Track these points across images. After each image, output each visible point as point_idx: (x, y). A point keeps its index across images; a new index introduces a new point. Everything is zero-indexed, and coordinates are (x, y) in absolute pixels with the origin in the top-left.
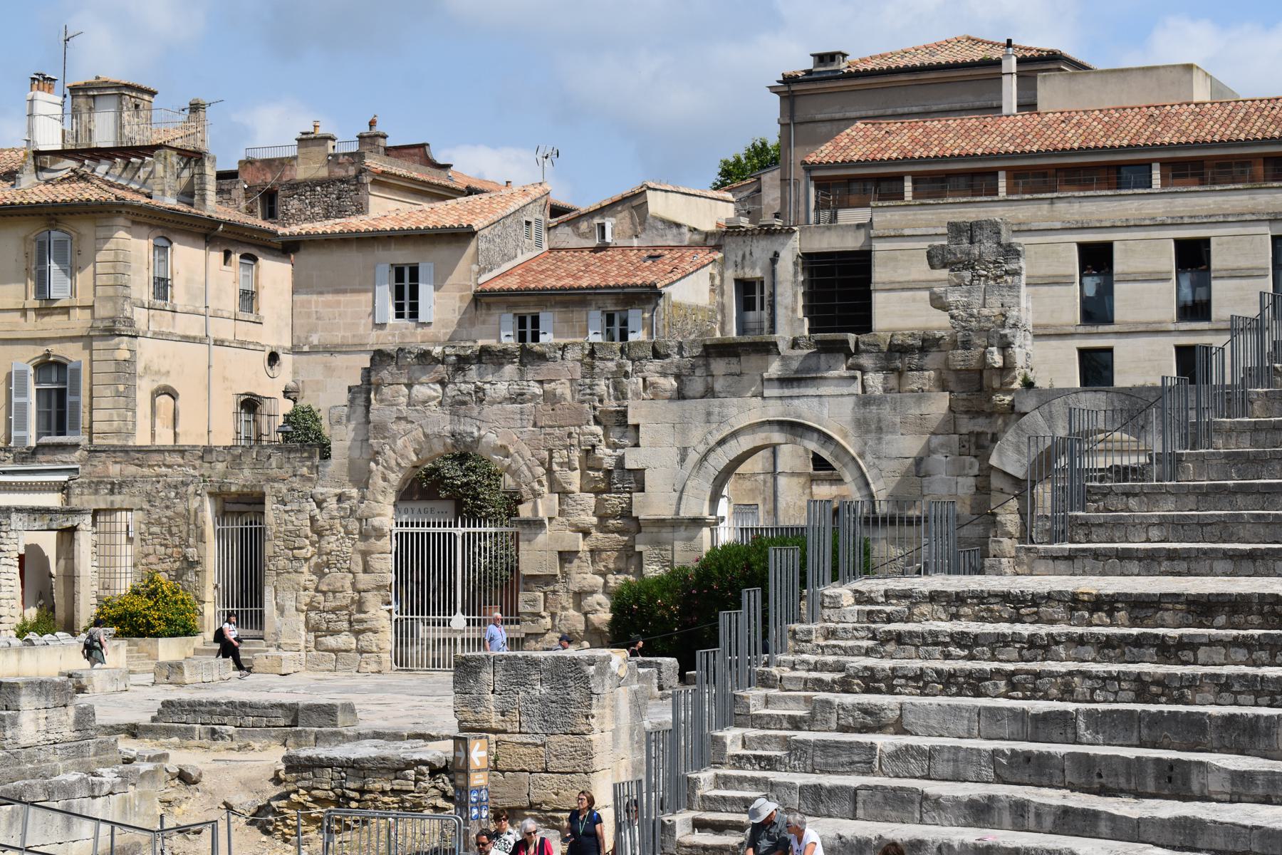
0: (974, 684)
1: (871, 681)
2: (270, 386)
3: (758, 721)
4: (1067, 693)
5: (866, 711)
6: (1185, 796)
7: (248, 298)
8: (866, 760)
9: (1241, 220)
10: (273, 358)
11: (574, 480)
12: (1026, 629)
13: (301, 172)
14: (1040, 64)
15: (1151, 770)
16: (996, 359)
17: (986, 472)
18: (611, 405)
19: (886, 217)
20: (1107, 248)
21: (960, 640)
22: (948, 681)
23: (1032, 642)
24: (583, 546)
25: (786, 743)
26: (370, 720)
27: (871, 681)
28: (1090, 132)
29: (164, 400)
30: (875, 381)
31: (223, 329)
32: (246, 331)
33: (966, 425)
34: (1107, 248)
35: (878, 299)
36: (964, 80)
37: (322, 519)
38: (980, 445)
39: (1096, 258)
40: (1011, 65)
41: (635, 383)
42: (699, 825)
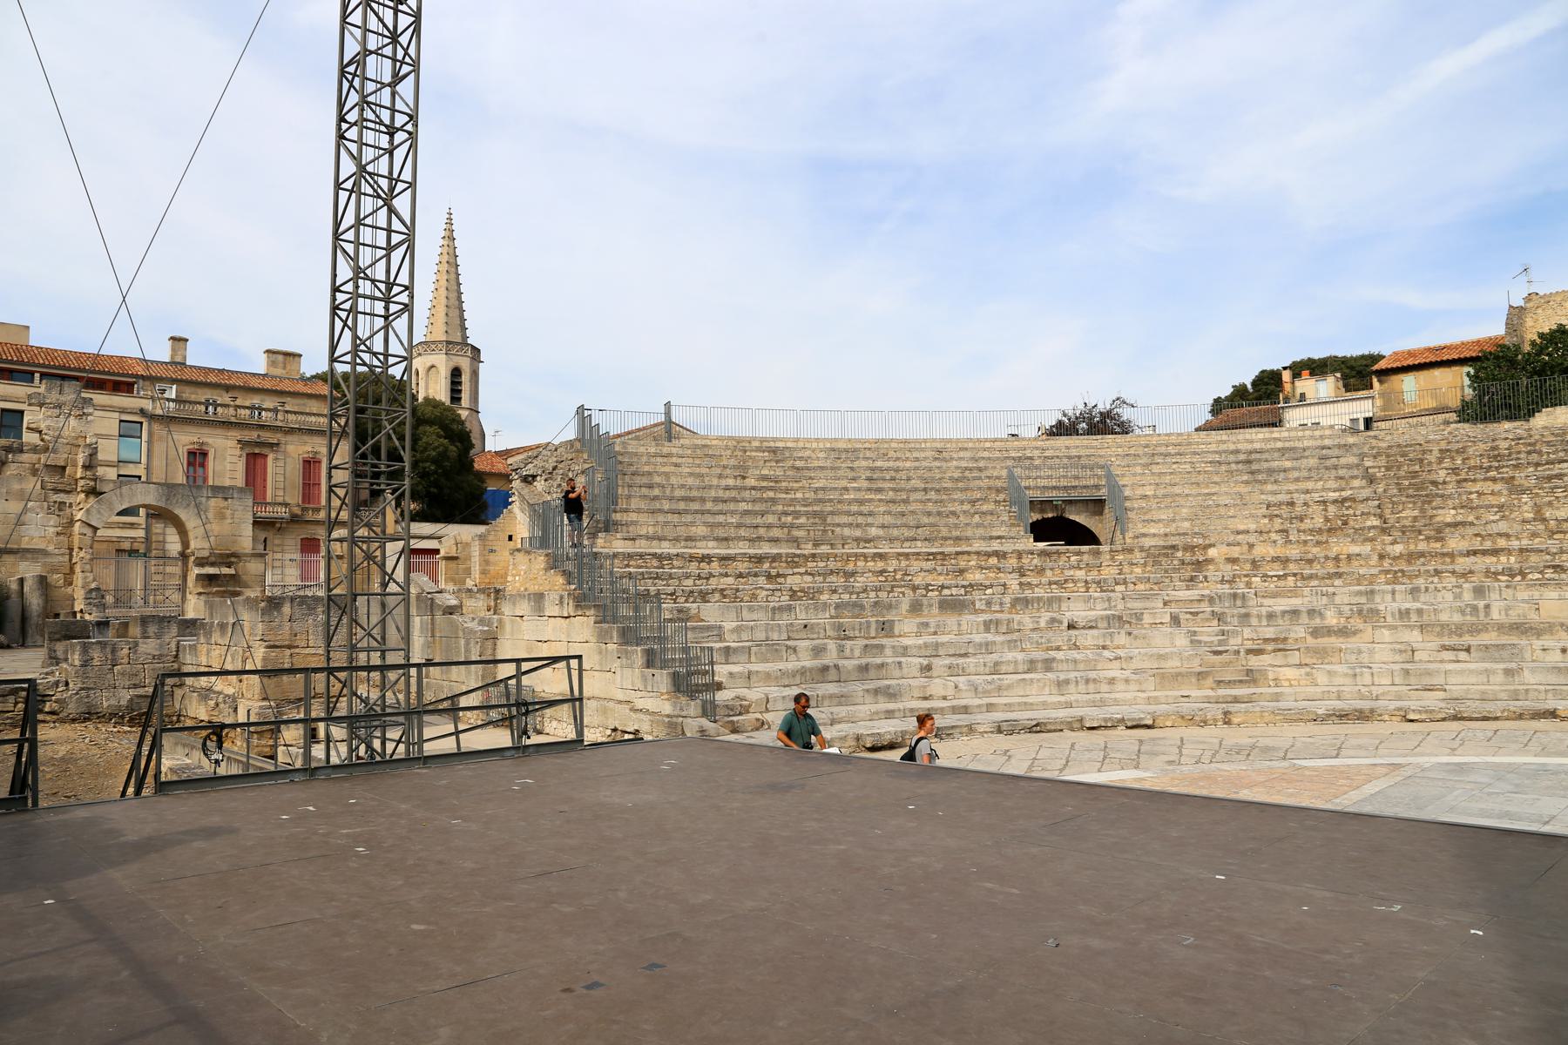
15: (873, 626)
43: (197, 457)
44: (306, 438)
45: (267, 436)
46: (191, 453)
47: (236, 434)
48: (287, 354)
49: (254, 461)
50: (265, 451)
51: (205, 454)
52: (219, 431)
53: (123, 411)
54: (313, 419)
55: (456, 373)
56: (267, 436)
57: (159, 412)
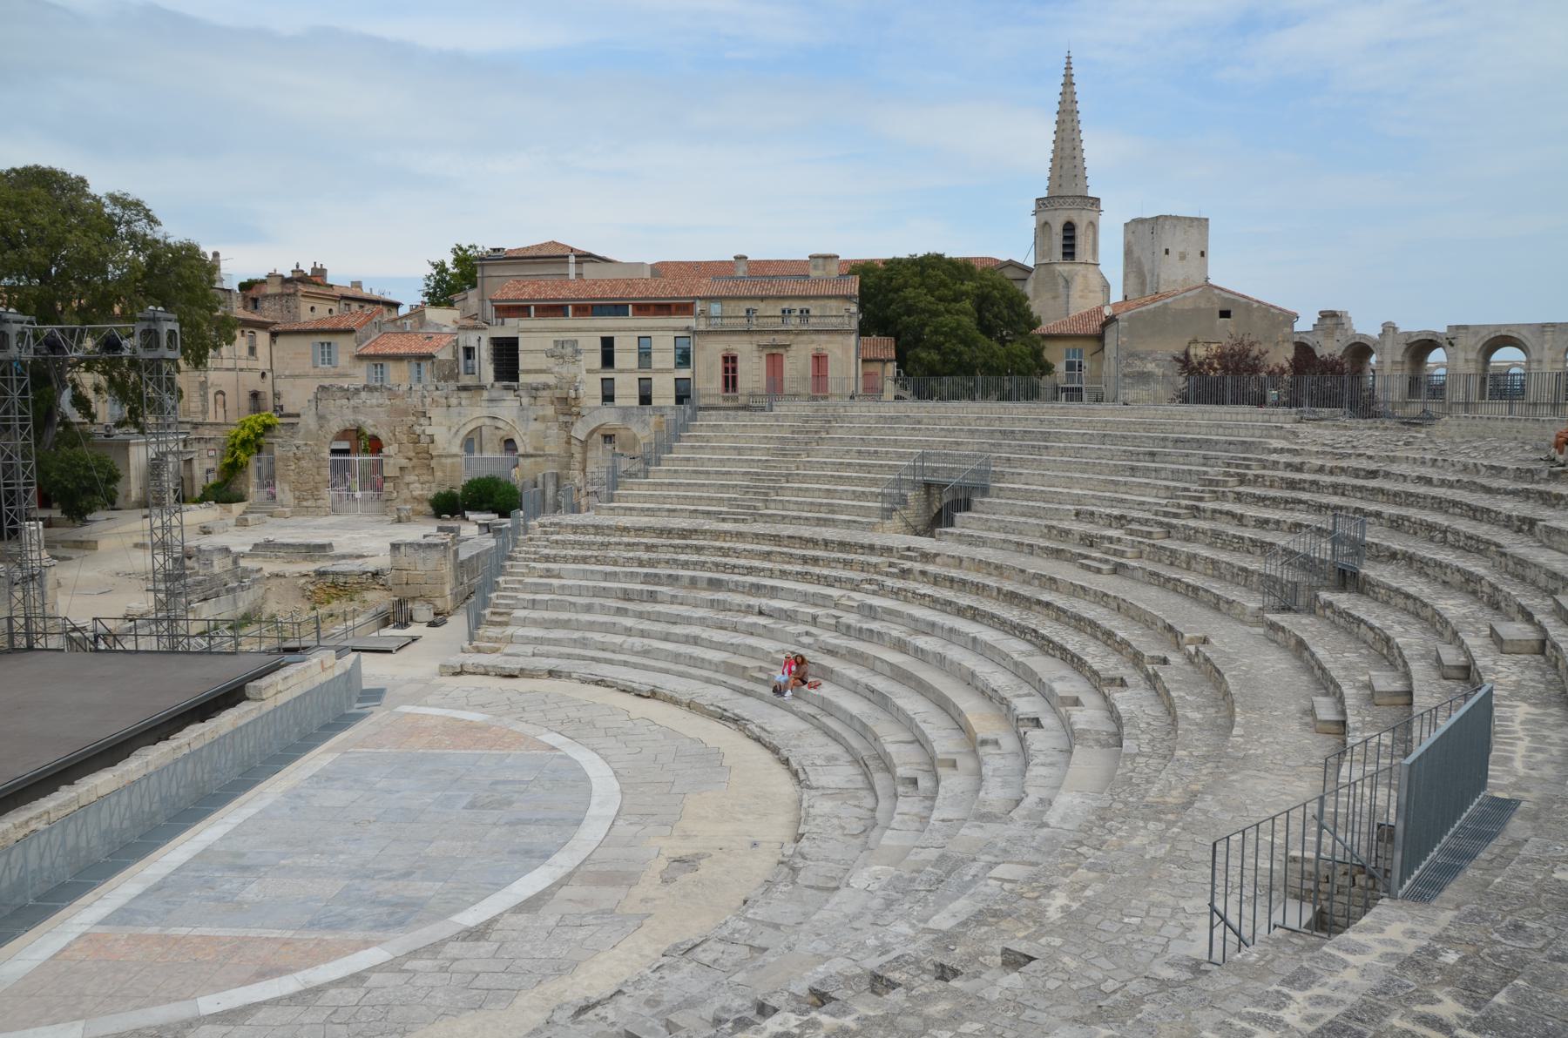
0: (585, 560)
1: (547, 559)
2: (265, 387)
3: (511, 574)
4: (615, 563)
5: (548, 570)
6: (656, 601)
7: (252, 350)
8: (550, 589)
9: (663, 329)
10: (263, 375)
11: (404, 439)
12: (599, 539)
13: (270, 290)
14: (585, 258)
16: (572, 393)
17: (570, 438)
18: (420, 409)
19: (525, 323)
20: (612, 338)
21: (576, 542)
22: (575, 560)
23: (602, 544)
24: (410, 465)
25: (520, 582)
26: (337, 551)
27: (547, 559)
28: (604, 291)
29: (220, 397)
30: (525, 400)
31: (242, 364)
32: (252, 364)
33: (562, 418)
34: (612, 338)
35: (521, 356)
36: (550, 258)
37: (299, 453)
38: (567, 426)
39: (608, 344)
40: (572, 259)
41: (428, 400)
42: (493, 613)
43: (730, 362)
44: (814, 337)
45: (780, 339)
46: (726, 359)
47: (757, 338)
48: (826, 257)
49: (774, 360)
50: (781, 351)
51: (734, 359)
52: (746, 338)
53: (675, 330)
54: (827, 320)
55: (1069, 228)
56: (780, 339)
57: (702, 328)
